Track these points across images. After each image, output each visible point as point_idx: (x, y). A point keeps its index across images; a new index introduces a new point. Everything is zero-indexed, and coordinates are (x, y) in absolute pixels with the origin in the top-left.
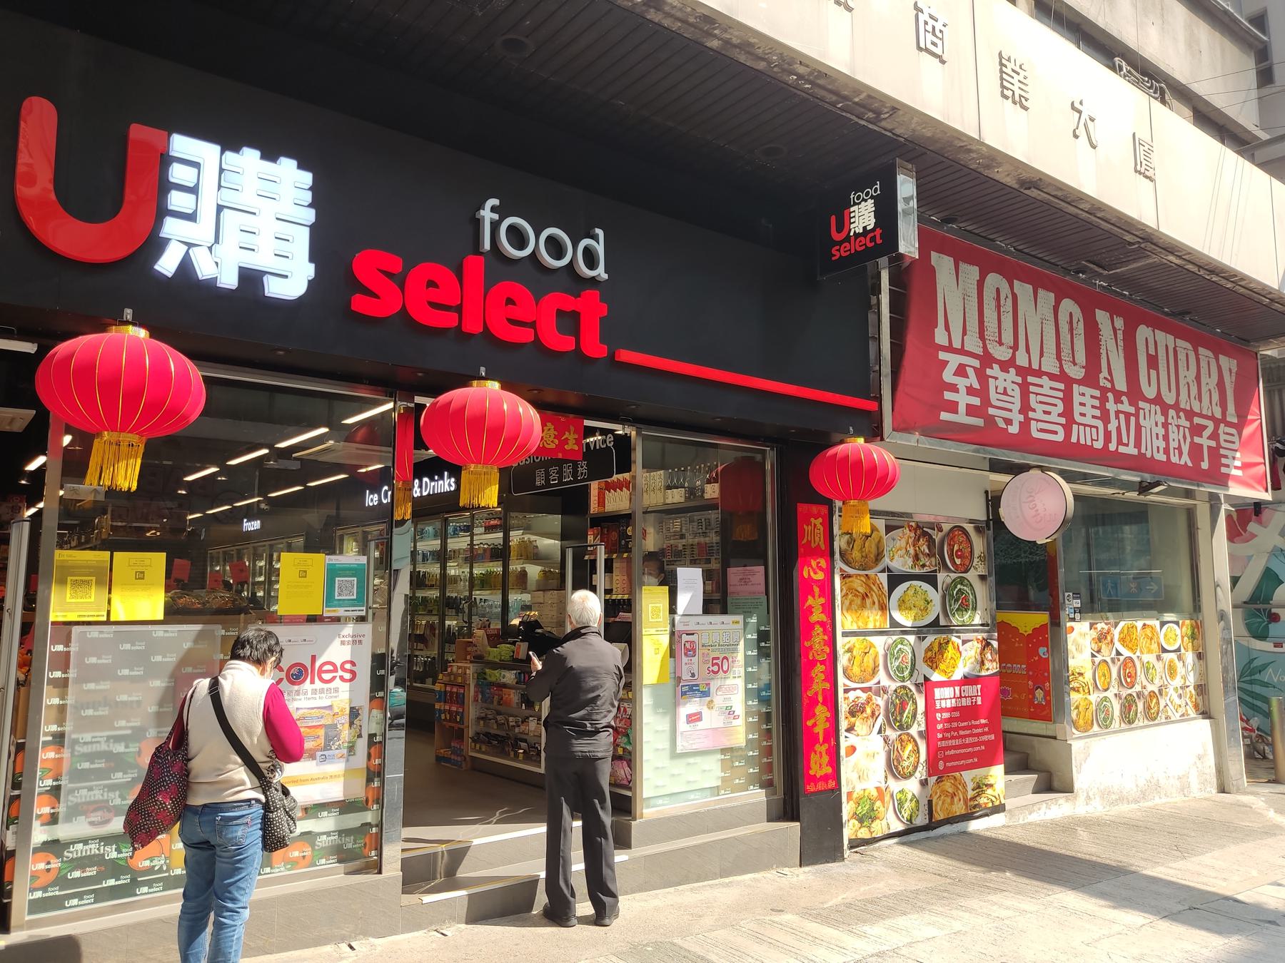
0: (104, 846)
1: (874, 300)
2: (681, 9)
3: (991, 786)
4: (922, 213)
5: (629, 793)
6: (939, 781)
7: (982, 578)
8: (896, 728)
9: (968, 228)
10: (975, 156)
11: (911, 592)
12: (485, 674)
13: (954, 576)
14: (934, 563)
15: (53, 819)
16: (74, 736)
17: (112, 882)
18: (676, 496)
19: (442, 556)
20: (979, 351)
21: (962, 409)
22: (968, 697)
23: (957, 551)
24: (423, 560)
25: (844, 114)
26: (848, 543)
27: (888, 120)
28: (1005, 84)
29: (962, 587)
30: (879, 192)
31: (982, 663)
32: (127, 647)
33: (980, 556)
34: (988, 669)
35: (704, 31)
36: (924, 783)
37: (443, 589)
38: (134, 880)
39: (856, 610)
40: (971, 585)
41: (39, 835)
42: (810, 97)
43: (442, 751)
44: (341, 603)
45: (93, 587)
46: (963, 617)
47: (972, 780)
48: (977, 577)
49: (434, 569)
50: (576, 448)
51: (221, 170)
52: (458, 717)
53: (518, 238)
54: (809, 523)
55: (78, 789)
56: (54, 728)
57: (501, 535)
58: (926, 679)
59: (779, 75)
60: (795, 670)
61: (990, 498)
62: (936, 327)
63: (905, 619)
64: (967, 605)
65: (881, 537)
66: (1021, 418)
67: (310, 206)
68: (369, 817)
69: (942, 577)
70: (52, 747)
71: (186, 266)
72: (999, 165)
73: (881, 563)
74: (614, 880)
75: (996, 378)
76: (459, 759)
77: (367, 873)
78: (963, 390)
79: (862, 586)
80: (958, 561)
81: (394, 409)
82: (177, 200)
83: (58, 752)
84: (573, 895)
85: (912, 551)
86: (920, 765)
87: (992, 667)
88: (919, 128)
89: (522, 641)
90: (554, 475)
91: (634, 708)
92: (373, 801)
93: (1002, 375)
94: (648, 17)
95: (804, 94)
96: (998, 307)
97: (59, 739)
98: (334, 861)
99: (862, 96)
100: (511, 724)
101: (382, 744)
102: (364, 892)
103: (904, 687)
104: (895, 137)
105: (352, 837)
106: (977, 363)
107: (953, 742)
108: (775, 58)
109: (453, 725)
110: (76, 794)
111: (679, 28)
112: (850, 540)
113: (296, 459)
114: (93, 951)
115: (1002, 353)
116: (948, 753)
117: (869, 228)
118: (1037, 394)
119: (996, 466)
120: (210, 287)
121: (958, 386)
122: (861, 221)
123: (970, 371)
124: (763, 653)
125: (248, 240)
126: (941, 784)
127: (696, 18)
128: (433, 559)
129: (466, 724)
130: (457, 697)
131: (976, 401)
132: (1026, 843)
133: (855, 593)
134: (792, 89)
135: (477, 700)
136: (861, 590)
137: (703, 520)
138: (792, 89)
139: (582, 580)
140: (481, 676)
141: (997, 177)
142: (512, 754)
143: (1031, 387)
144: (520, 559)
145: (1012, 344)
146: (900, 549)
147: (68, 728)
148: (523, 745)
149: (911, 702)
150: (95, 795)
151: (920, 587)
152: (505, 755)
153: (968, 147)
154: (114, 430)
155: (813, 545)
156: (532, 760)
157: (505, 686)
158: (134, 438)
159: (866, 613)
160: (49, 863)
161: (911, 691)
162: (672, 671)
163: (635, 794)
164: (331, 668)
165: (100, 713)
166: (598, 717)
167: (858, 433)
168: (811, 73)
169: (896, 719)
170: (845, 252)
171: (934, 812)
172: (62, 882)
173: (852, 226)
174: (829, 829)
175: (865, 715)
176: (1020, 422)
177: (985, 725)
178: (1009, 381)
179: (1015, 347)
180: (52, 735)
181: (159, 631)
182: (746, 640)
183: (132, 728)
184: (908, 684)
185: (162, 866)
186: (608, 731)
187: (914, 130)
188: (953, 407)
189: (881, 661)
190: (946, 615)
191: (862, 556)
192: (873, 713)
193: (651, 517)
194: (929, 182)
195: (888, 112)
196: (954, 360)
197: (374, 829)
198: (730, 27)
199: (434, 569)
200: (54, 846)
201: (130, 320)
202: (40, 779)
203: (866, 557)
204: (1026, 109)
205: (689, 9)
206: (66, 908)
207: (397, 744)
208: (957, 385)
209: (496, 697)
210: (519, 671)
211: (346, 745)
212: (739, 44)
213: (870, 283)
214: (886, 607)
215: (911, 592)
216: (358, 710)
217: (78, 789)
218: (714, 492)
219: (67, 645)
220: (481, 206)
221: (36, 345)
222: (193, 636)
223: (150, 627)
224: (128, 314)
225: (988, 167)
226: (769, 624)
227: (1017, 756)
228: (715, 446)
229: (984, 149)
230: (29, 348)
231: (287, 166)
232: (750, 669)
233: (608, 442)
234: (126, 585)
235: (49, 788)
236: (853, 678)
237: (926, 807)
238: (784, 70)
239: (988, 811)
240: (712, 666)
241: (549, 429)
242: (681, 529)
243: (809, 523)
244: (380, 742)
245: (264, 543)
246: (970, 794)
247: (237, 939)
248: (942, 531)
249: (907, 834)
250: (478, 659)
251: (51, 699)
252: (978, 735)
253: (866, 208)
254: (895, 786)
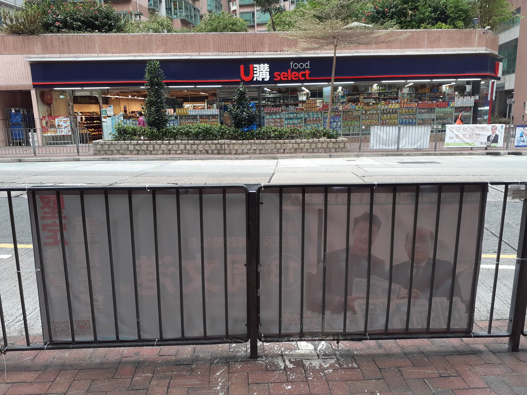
71: (257, 79)
125: (262, 75)
231: (266, 64)
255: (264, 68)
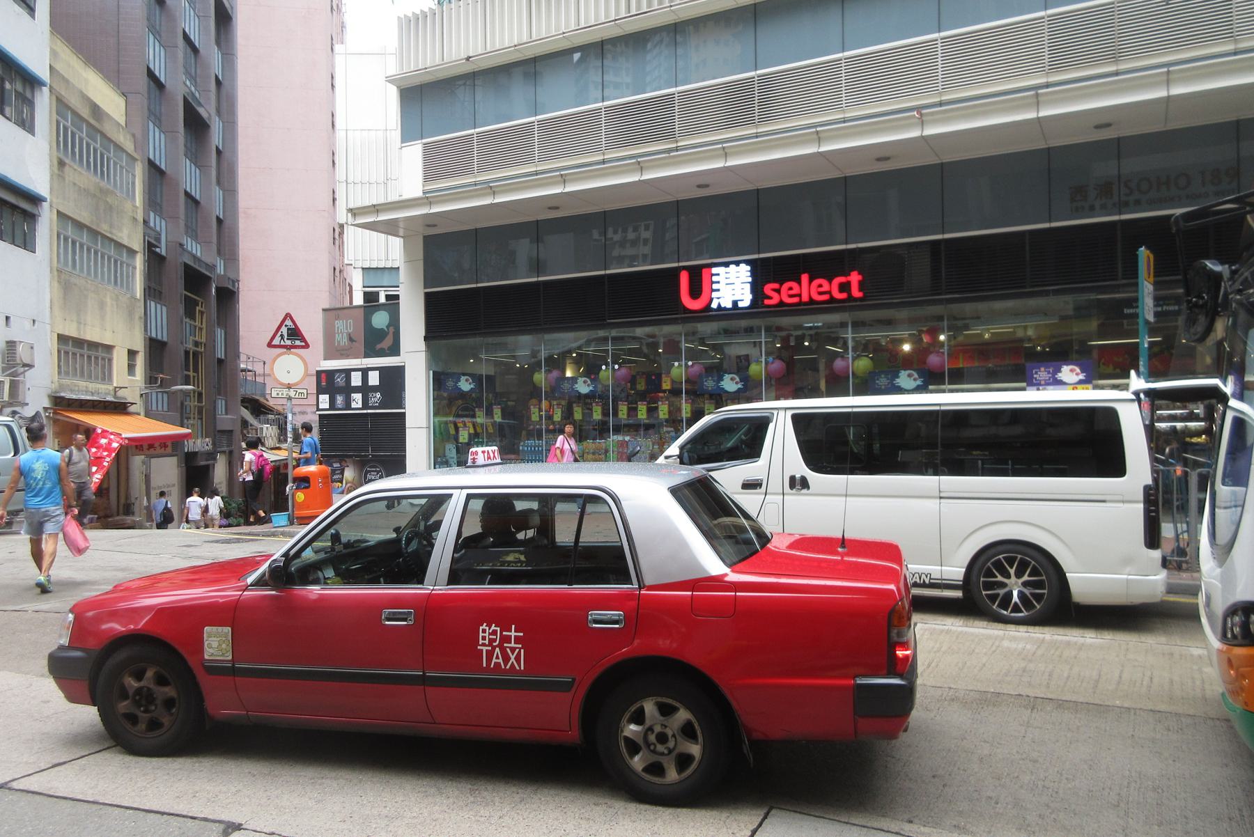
71: (719, 305)
255: (738, 275)
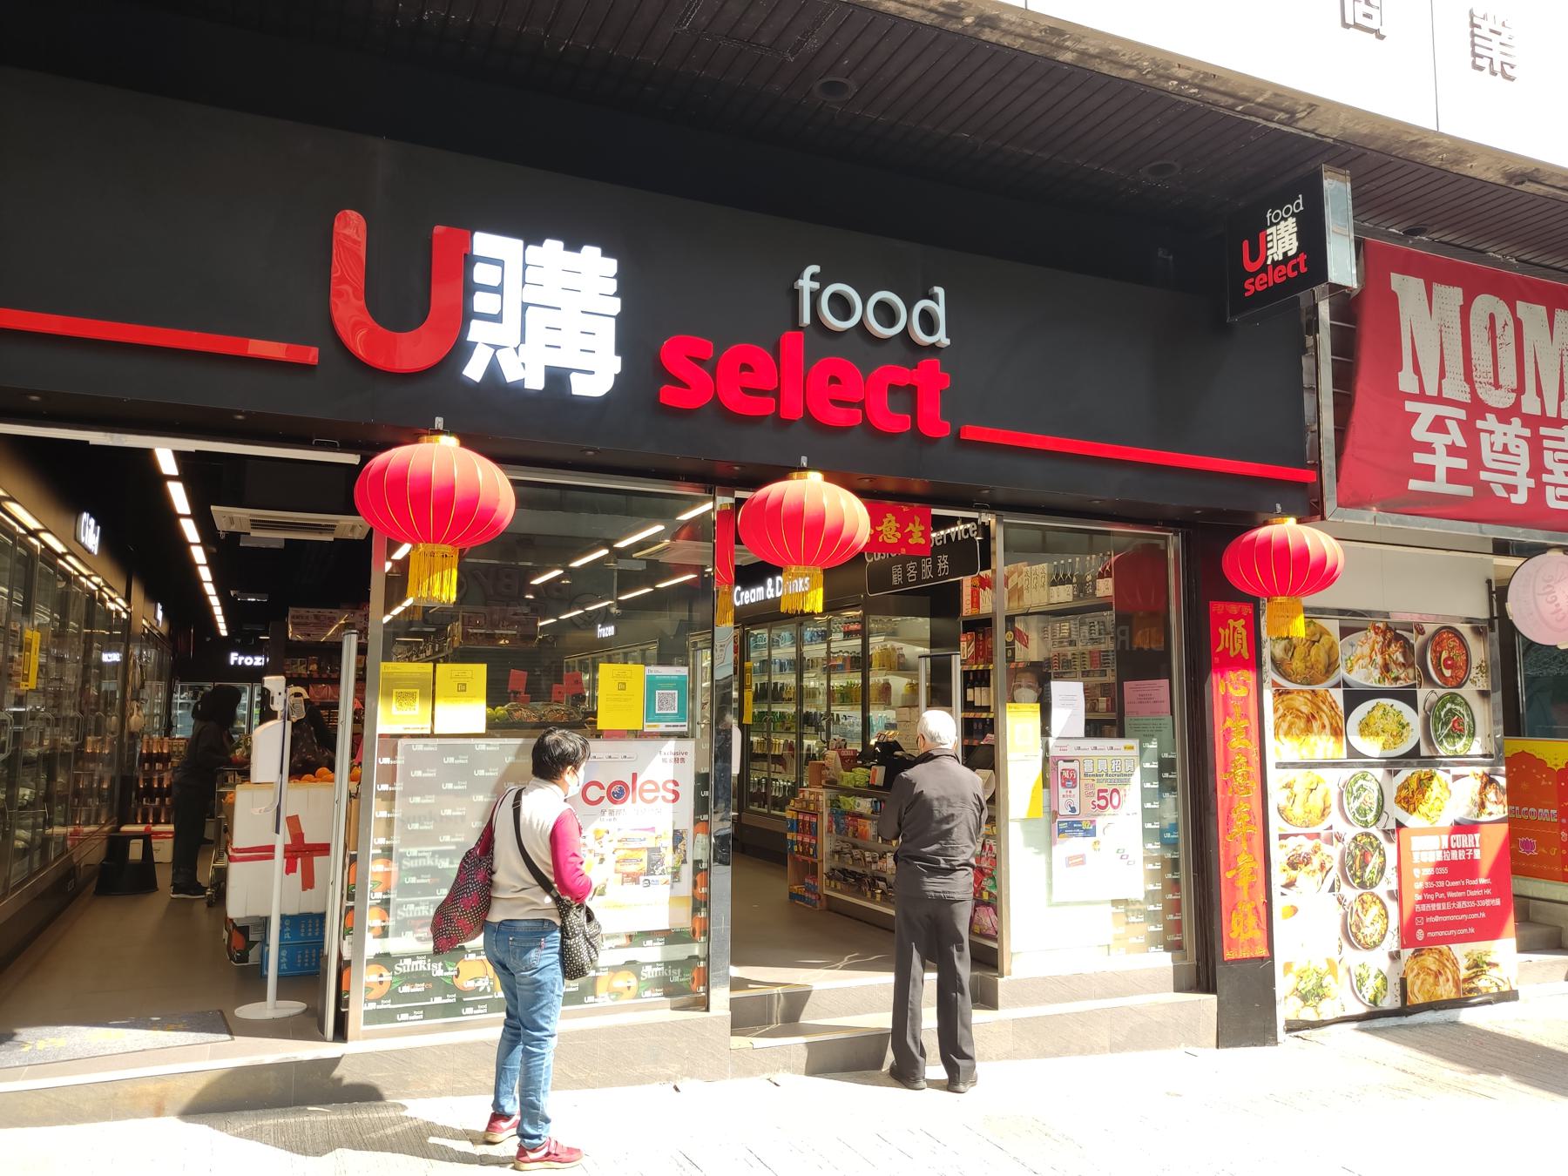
0: (431, 962)
1: (1309, 341)
2: (1021, 25)
3: (1496, 965)
4: (1376, 225)
5: (995, 945)
6: (1418, 954)
7: (1484, 694)
8: (1355, 885)
9: (1446, 239)
10: (1436, 151)
11: (1377, 713)
12: (839, 801)
13: (1441, 692)
14: (1411, 676)
15: (384, 933)
16: (401, 850)
17: (438, 1000)
18: (1063, 595)
19: (800, 665)
20: (1466, 398)
21: (1440, 474)
22: (1461, 848)
23: (1445, 660)
24: (781, 670)
25: (1247, 118)
26: (1286, 650)
27: (1307, 119)
28: (1478, 50)
29: (1453, 707)
30: (1301, 208)
31: (1482, 805)
32: (451, 760)
33: (1480, 666)
34: (1490, 814)
35: (1052, 45)
36: (1395, 957)
37: (800, 703)
38: (459, 1000)
39: (1297, 735)
40: (1466, 704)
41: (372, 946)
42: (1199, 103)
43: (796, 887)
44: (662, 718)
45: (418, 699)
46: (1455, 746)
47: (1466, 956)
48: (1476, 694)
49: (789, 680)
50: (922, 541)
51: (525, 266)
52: (811, 850)
53: (842, 306)
54: (1226, 626)
55: (406, 903)
56: (382, 841)
57: (859, 642)
58: (1400, 825)
59: (1154, 82)
60: (1208, 808)
61: (1494, 589)
62: (1401, 370)
63: (1371, 747)
64: (1460, 730)
65: (1333, 642)
66: (1531, 483)
67: (616, 295)
68: (697, 949)
69: (1423, 693)
70: (380, 860)
71: (493, 370)
72: (1473, 158)
73: (1334, 675)
74: (971, 1042)
75: (1491, 432)
76: (814, 897)
77: (694, 1010)
78: (1441, 451)
79: (1306, 704)
80: (1447, 673)
81: (713, 509)
82: (482, 302)
83: (387, 865)
84: (923, 1054)
85: (1379, 659)
86: (1388, 933)
87: (1497, 809)
88: (1350, 125)
89: (878, 764)
90: (912, 571)
91: (999, 847)
92: (700, 933)
93: (1500, 428)
94: (984, 38)
95: (1190, 100)
96: (1493, 338)
97: (388, 852)
98: (660, 994)
99: (1267, 95)
100: (867, 859)
101: (708, 871)
102: (691, 1029)
103: (1368, 835)
104: (1319, 138)
105: (679, 971)
106: (1461, 414)
107: (1439, 906)
108: (1145, 64)
109: (806, 858)
110: (404, 909)
111: (1022, 45)
112: (1288, 646)
113: (640, 559)
114: (422, 1066)
115: (1500, 399)
116: (1430, 919)
117: (1290, 254)
118: (1555, 450)
119: (1501, 548)
120: (517, 389)
121: (1433, 446)
122: (1280, 246)
123: (1452, 426)
124: (1166, 786)
125: (553, 337)
126: (1419, 959)
127: (1041, 32)
128: (790, 669)
129: (819, 858)
130: (809, 827)
131: (1461, 464)
132: (1545, 1044)
133: (1298, 714)
134: (1173, 96)
135: (831, 832)
136: (1306, 709)
137: (1096, 623)
138: (1173, 96)
139: (939, 697)
140: (834, 803)
141: (1472, 173)
142: (869, 894)
143: (1544, 441)
144: (883, 670)
145: (1515, 386)
146: (1362, 657)
147: (395, 842)
148: (882, 884)
149: (1377, 853)
150: (421, 911)
151: (1392, 706)
152: (862, 895)
153: (1424, 141)
154: (428, 541)
155: (1232, 654)
156: (890, 902)
157: (861, 816)
158: (447, 548)
159: (1312, 739)
160: (381, 976)
161: (1376, 839)
162: (1047, 804)
163: (1001, 945)
164: (653, 787)
165: (426, 827)
166: (954, 852)
167: (1287, 512)
168: (1194, 76)
169: (1355, 874)
170: (1261, 285)
171: (1409, 994)
172: (393, 995)
173: (1269, 252)
174: (1257, 1005)
175: (1309, 867)
176: (1528, 488)
177: (1485, 886)
178: (1511, 436)
179: (1520, 390)
180: (381, 848)
181: (481, 745)
182: (1143, 769)
183: (456, 844)
184: (1373, 830)
185: (486, 988)
186: (966, 870)
187: (1343, 128)
188: (1427, 473)
189: (1333, 801)
190: (1430, 742)
191: (1306, 667)
192: (1322, 866)
193: (1033, 620)
194: (1378, 188)
195: (1305, 111)
196: (1428, 412)
197: (702, 963)
198: (1084, 37)
199: (789, 680)
200: (385, 959)
201: (441, 429)
202: (371, 891)
203: (1312, 668)
204: (1511, 79)
205: (1031, 23)
206: (397, 1021)
207: (722, 877)
208: (1432, 443)
209: (851, 828)
210: (875, 799)
211: (670, 870)
212: (1098, 53)
213: (1304, 320)
214: (1341, 731)
215: (1377, 713)
216: (681, 834)
217: (406, 903)
218: (1107, 589)
219: (394, 758)
220: (799, 276)
221: (359, 456)
222: (514, 750)
223: (472, 741)
224: (439, 422)
225: (1457, 162)
226: (1175, 751)
227: (1545, 930)
228: (1108, 533)
229: (1446, 141)
230: (353, 459)
231: (591, 253)
232: (1148, 805)
233: (971, 532)
234: (447, 696)
235: (379, 901)
236: (1294, 821)
237: (1398, 987)
238: (1160, 76)
239: (1491, 998)
240: (1099, 800)
241: (890, 521)
242: (1070, 633)
243: (1226, 626)
244: (706, 870)
245: (601, 654)
246: (1464, 974)
247: (547, 1067)
248: (1423, 633)
249: (1371, 1017)
250: (832, 784)
251: (379, 812)
252: (1475, 898)
253: (1286, 229)
254: (1353, 957)
255: (572, 281)
